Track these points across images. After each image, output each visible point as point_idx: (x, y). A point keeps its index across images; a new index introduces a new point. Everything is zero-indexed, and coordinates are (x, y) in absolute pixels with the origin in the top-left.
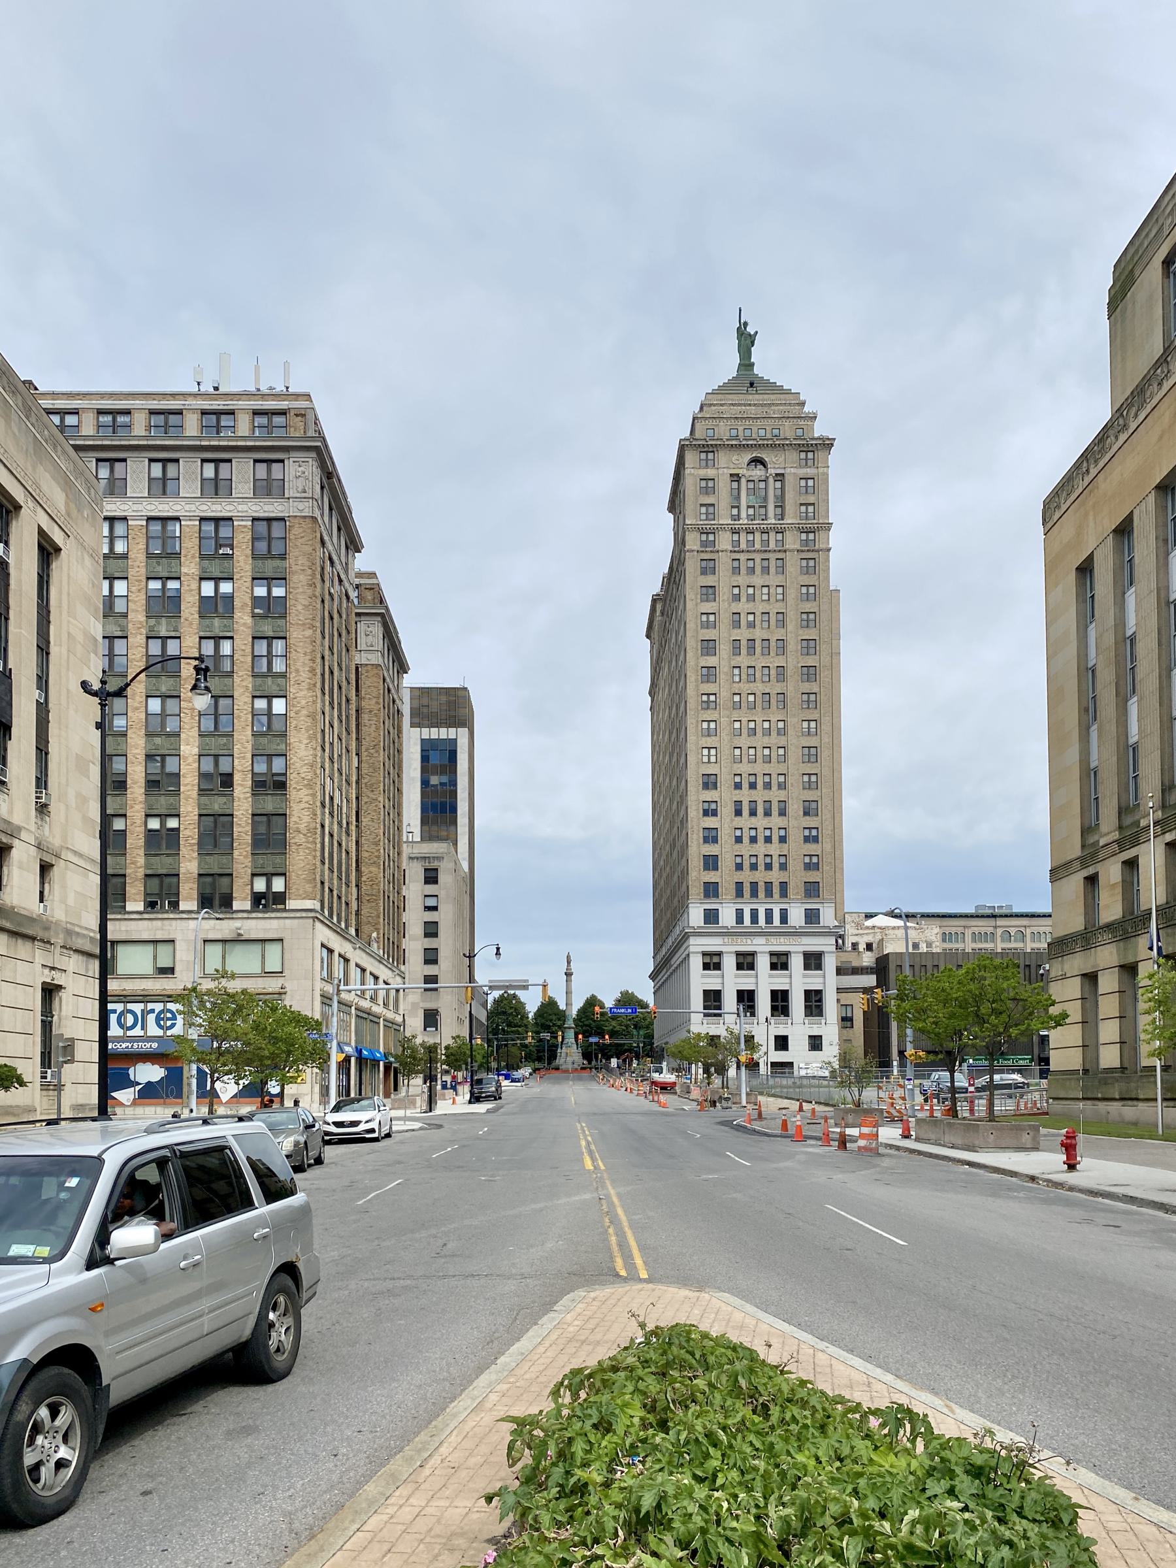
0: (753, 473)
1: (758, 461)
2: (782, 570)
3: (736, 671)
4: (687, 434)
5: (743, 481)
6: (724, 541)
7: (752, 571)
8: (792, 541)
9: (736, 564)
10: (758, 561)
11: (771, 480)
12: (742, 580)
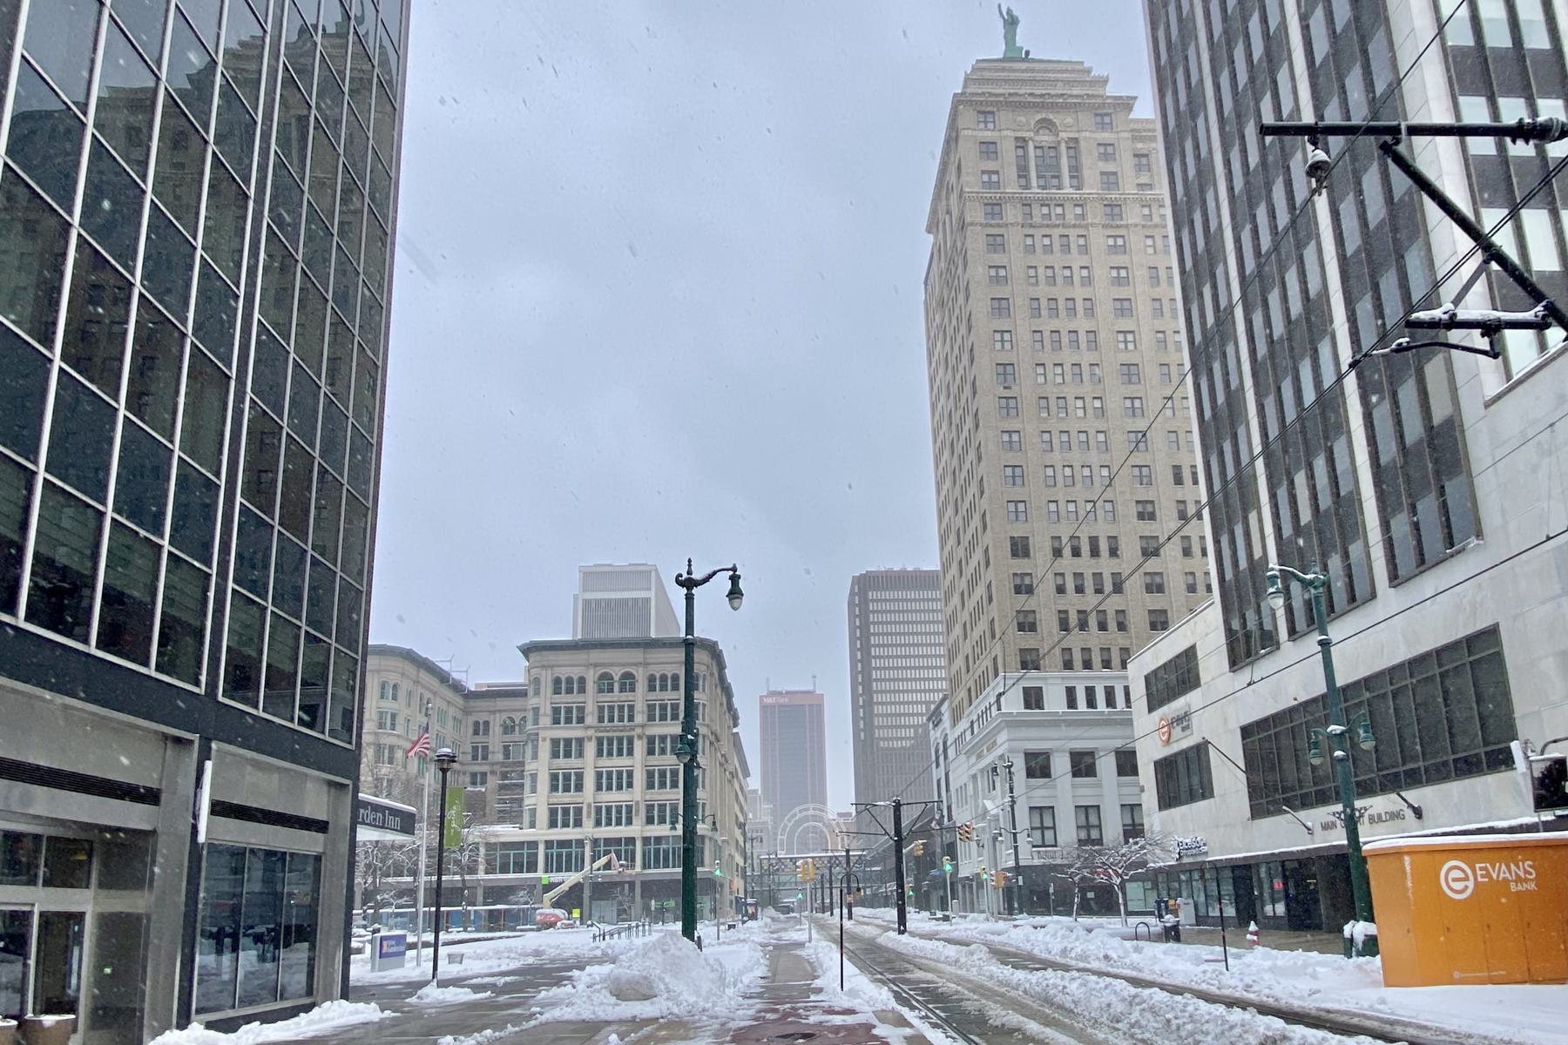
1: (1047, 125)
2: (1084, 250)
3: (1040, 370)
5: (1031, 145)
7: (1048, 249)
8: (1095, 215)
9: (1029, 241)
11: (1063, 147)
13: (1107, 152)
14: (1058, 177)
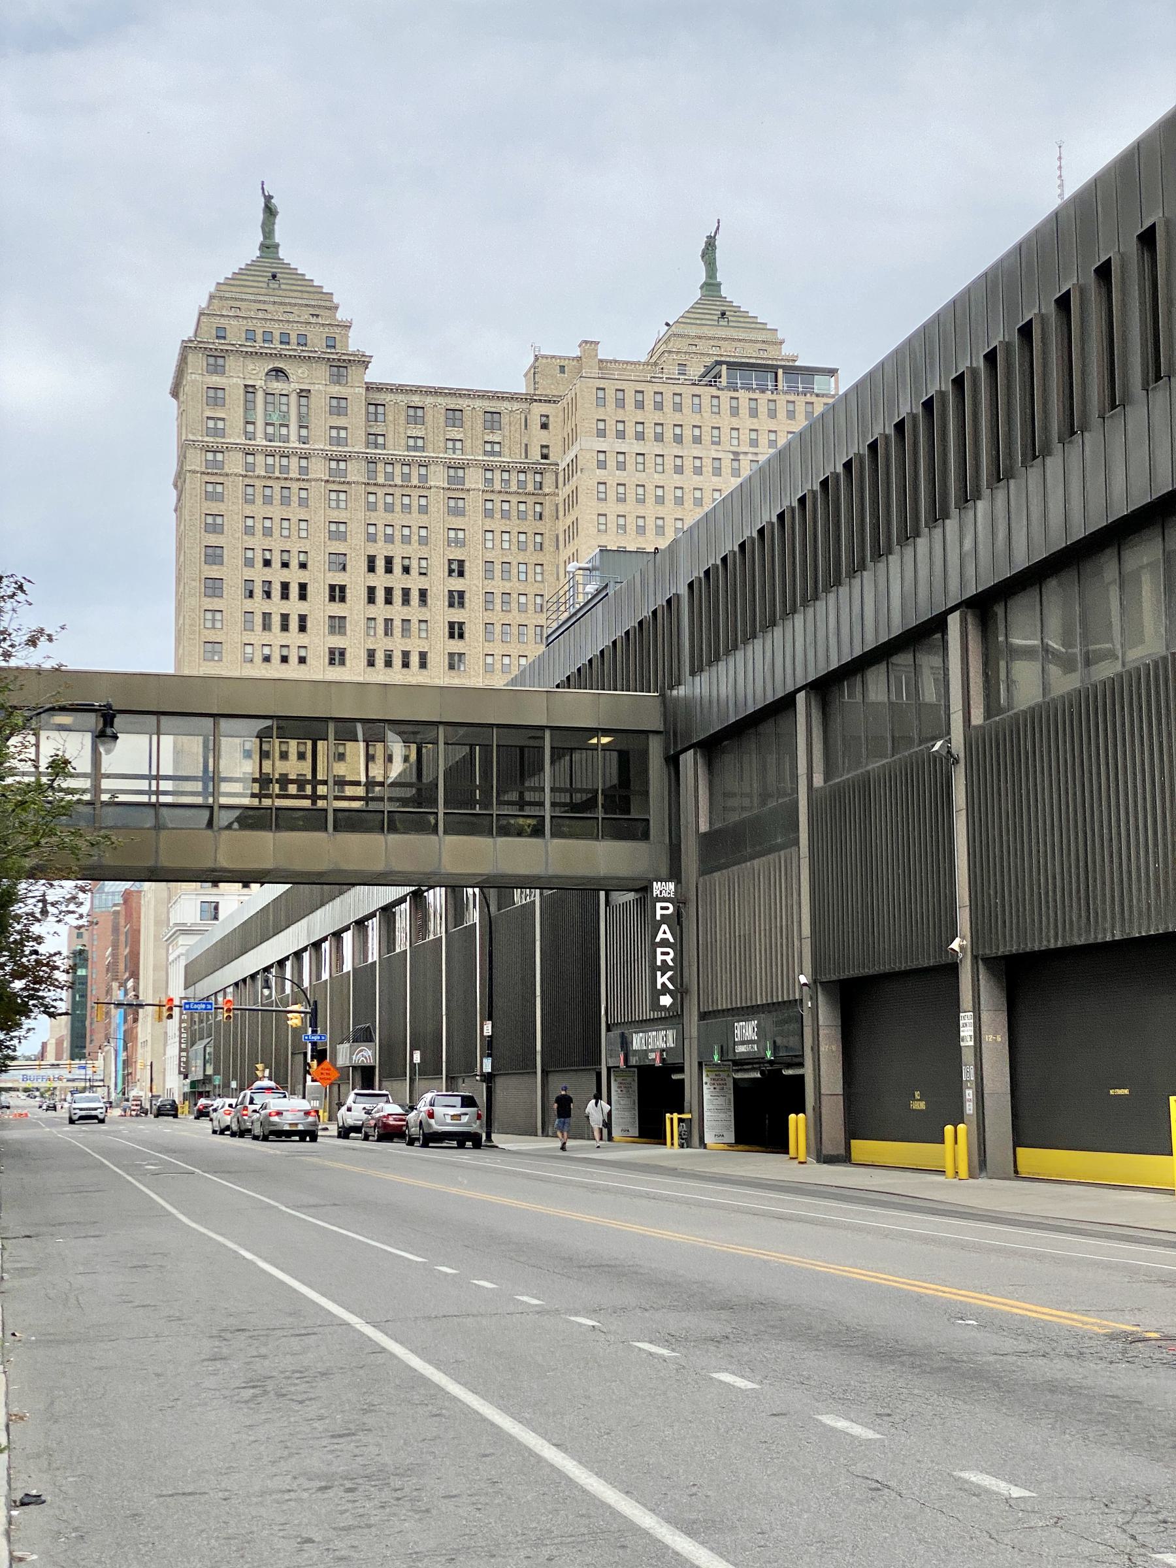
0: (275, 385)
1: (278, 373)
2: (303, 503)
4: (191, 333)
5: (260, 395)
6: (234, 463)
7: (268, 500)
10: (277, 489)
12: (259, 510)
13: (339, 406)
14: (287, 426)
